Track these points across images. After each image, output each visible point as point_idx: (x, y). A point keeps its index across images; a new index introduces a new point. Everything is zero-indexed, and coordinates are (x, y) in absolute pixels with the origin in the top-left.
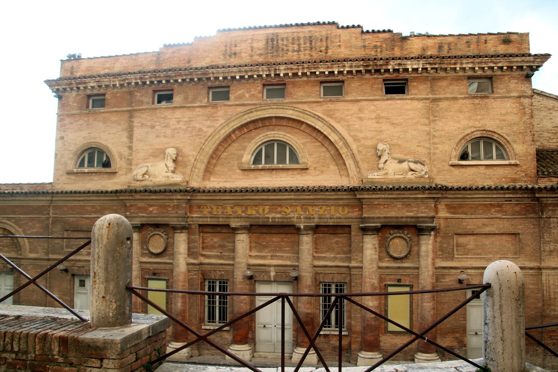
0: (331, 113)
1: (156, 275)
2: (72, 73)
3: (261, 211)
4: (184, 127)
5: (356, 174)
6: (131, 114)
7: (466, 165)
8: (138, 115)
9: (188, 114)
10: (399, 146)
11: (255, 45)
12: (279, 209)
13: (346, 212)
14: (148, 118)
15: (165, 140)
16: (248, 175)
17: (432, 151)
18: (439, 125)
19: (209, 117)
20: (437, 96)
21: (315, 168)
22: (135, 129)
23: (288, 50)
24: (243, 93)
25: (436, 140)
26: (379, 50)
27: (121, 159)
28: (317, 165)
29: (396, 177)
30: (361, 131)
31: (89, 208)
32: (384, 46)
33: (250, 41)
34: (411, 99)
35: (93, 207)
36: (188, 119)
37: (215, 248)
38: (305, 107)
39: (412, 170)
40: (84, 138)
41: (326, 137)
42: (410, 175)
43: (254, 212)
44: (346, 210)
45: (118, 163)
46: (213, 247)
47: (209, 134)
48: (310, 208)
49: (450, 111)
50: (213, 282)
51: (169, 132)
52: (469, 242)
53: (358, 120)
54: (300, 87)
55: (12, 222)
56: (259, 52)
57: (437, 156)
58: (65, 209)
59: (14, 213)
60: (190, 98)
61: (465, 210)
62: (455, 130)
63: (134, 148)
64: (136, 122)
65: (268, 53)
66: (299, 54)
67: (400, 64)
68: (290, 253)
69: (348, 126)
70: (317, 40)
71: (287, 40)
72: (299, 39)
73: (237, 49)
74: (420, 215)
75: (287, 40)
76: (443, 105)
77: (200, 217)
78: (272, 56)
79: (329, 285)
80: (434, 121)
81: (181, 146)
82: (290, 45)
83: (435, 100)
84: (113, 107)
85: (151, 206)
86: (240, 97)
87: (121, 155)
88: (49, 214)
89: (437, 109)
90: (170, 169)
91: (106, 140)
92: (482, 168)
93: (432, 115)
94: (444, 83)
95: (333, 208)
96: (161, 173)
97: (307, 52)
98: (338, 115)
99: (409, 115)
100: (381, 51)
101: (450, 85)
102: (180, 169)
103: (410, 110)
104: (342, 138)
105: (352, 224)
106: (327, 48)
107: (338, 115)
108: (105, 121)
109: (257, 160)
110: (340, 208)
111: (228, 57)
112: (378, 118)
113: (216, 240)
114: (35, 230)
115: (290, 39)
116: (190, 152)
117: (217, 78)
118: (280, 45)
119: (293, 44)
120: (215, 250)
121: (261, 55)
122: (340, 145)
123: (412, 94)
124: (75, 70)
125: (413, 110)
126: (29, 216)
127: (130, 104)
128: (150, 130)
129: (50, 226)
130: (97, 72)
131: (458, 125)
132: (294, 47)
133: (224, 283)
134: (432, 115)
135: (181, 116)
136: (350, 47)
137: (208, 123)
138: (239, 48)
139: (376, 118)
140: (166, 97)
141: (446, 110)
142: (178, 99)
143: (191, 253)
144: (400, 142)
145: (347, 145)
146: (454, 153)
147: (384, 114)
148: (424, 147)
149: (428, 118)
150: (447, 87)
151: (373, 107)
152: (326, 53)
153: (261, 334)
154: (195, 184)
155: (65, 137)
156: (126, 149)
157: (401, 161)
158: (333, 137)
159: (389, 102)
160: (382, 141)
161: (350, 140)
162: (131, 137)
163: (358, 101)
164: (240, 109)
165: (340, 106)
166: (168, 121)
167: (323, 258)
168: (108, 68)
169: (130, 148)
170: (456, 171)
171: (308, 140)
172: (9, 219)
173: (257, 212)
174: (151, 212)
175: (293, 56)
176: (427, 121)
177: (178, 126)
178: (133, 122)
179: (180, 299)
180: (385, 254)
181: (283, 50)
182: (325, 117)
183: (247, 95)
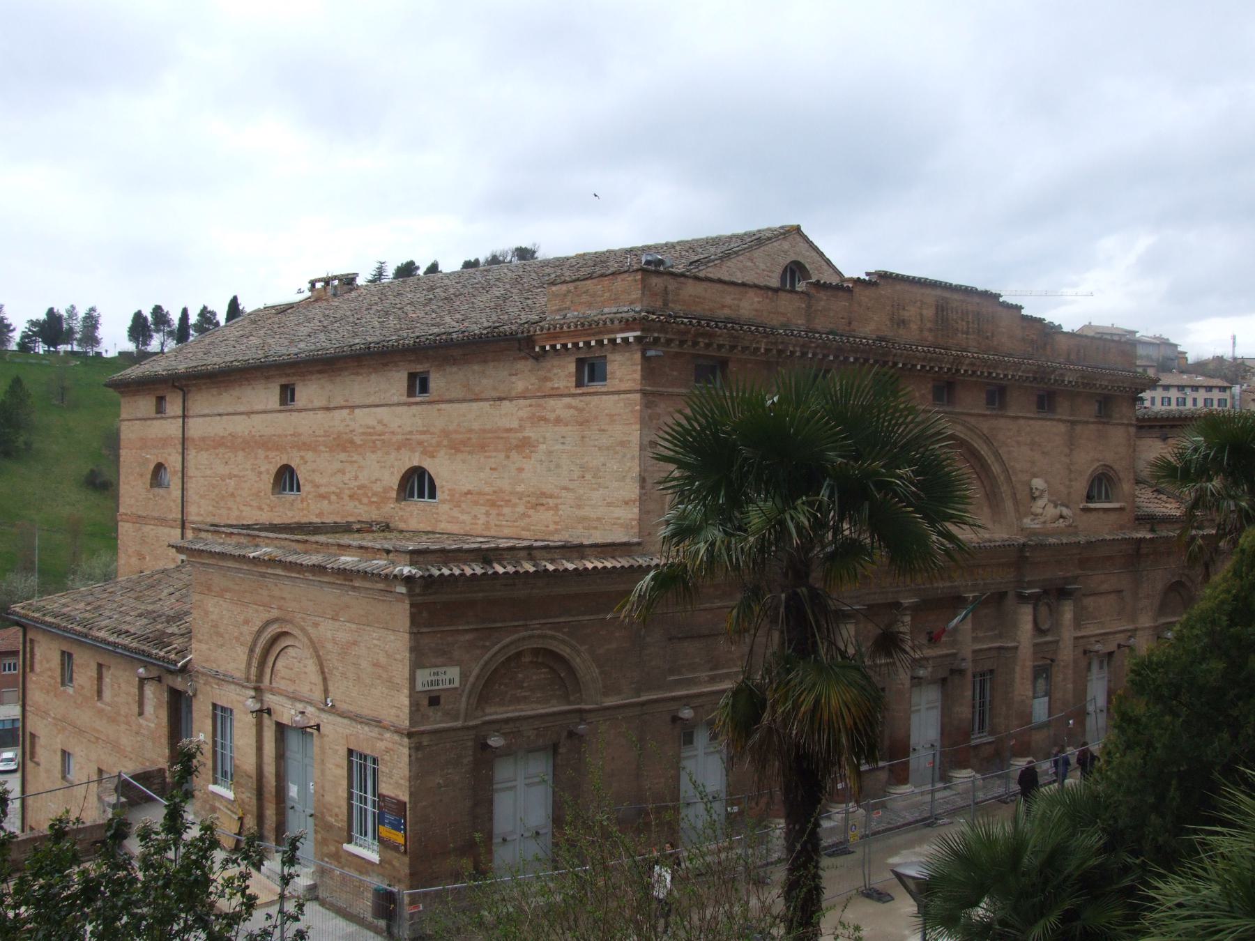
2: (665, 304)
11: (925, 312)
34: (1059, 420)
38: (972, 421)
39: (1061, 517)
55: (564, 633)
56: (929, 325)
73: (906, 314)
83: (1073, 423)
92: (1101, 514)
93: (1071, 443)
117: (895, 364)
121: (930, 330)
124: (670, 297)
134: (1071, 443)
147: (1037, 439)
157: (1056, 506)
158: (996, 468)
159: (1040, 422)
160: (1035, 476)
163: (1017, 418)
165: (1002, 423)
168: (730, 307)
172: (556, 627)
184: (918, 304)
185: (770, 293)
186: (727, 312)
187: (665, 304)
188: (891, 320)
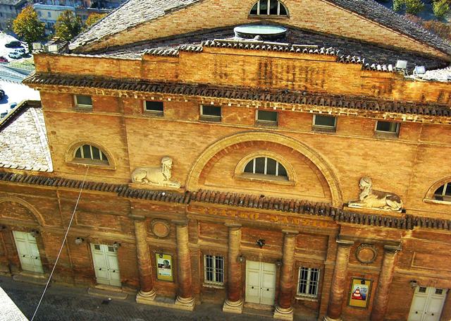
0: (322, 145)
1: (162, 251)
2: (49, 70)
3: (252, 216)
4: (177, 140)
5: (338, 198)
6: (122, 121)
7: (438, 204)
8: (129, 122)
9: (181, 128)
10: (382, 181)
11: (247, 68)
12: (268, 217)
13: (326, 226)
14: (140, 126)
15: (159, 149)
16: (240, 184)
17: (411, 188)
18: (422, 167)
19: (202, 133)
20: (425, 143)
21: (302, 186)
22: (128, 135)
23: (281, 79)
24: (235, 116)
25: (416, 180)
26: (377, 91)
27: (118, 159)
28: (304, 183)
29: (373, 209)
30: (348, 165)
31: (95, 196)
32: (383, 87)
33: (241, 63)
35: (98, 195)
36: (181, 133)
37: (211, 234)
40: (77, 136)
41: (312, 165)
42: (385, 209)
43: (246, 217)
44: (326, 224)
45: (117, 163)
46: (209, 233)
47: (202, 148)
48: (295, 220)
49: (435, 157)
50: (211, 257)
51: (162, 142)
52: (427, 258)
53: (346, 155)
54: (292, 118)
57: (414, 192)
58: (71, 194)
59: (23, 192)
60: (181, 113)
61: (428, 236)
62: (436, 173)
63: (130, 152)
64: (128, 128)
65: (260, 79)
66: (293, 85)
67: (394, 115)
68: (275, 244)
69: (336, 158)
70: (313, 72)
71: (282, 68)
72: (294, 68)
74: (388, 239)
75: (282, 68)
76: (429, 150)
77: (198, 215)
78: (265, 83)
79: (307, 269)
80: (417, 163)
81: (176, 156)
82: (284, 74)
84: (102, 111)
85: (154, 205)
86: (232, 119)
87: (118, 157)
88: (57, 196)
89: (423, 153)
90: (168, 178)
91: (99, 140)
93: (418, 156)
94: (436, 131)
95: (315, 222)
96: (160, 180)
97: (302, 83)
98: (328, 148)
99: (395, 156)
100: (379, 92)
101: (442, 133)
102: (177, 175)
103: (396, 152)
104: (329, 169)
105: (330, 235)
106: (323, 81)
107: (328, 148)
108: (95, 122)
109: (248, 169)
110: (321, 223)
111: (218, 77)
112: (365, 156)
113: (212, 228)
114: (47, 208)
115: (285, 68)
116: (184, 161)
118: (274, 72)
119: (288, 72)
120: (212, 236)
121: (253, 79)
122: (326, 174)
123: (402, 138)
125: (400, 152)
126: (38, 197)
127: (119, 110)
128: (143, 138)
129: (60, 206)
130: (76, 72)
131: (440, 170)
132: (288, 77)
133: (220, 258)
134: (418, 156)
135: (173, 129)
136: (347, 83)
137: (201, 139)
138: (231, 69)
139: (363, 155)
140: (157, 106)
141: (432, 156)
142: (168, 112)
143: (191, 239)
144: (382, 178)
145: (332, 174)
146: (429, 192)
147: (371, 153)
148: (403, 185)
149: (412, 162)
150: (437, 134)
151: (362, 145)
152: (322, 87)
153: (249, 291)
154: (193, 188)
155: (57, 132)
156: (121, 151)
157: (380, 197)
158: (321, 166)
161: (336, 171)
162: (124, 141)
164: (232, 131)
166: (160, 132)
167: (303, 252)
169: (126, 151)
170: (428, 207)
171: (296, 162)
172: (20, 197)
173: (249, 216)
174: (153, 209)
175: (287, 86)
176: (411, 164)
177: (171, 138)
178: (125, 127)
179: (185, 272)
180: (354, 258)
181: (277, 77)
182: (315, 150)
183: (239, 118)
184: (241, 63)
185: (115, 61)
186: (87, 72)
187: (49, 70)
188: (215, 73)
